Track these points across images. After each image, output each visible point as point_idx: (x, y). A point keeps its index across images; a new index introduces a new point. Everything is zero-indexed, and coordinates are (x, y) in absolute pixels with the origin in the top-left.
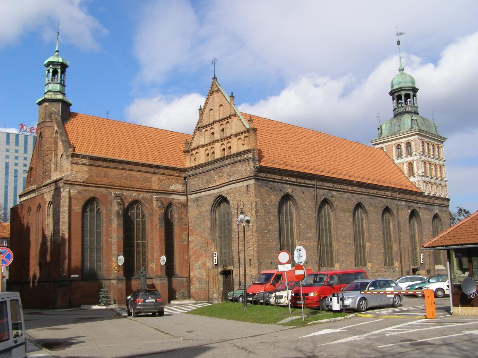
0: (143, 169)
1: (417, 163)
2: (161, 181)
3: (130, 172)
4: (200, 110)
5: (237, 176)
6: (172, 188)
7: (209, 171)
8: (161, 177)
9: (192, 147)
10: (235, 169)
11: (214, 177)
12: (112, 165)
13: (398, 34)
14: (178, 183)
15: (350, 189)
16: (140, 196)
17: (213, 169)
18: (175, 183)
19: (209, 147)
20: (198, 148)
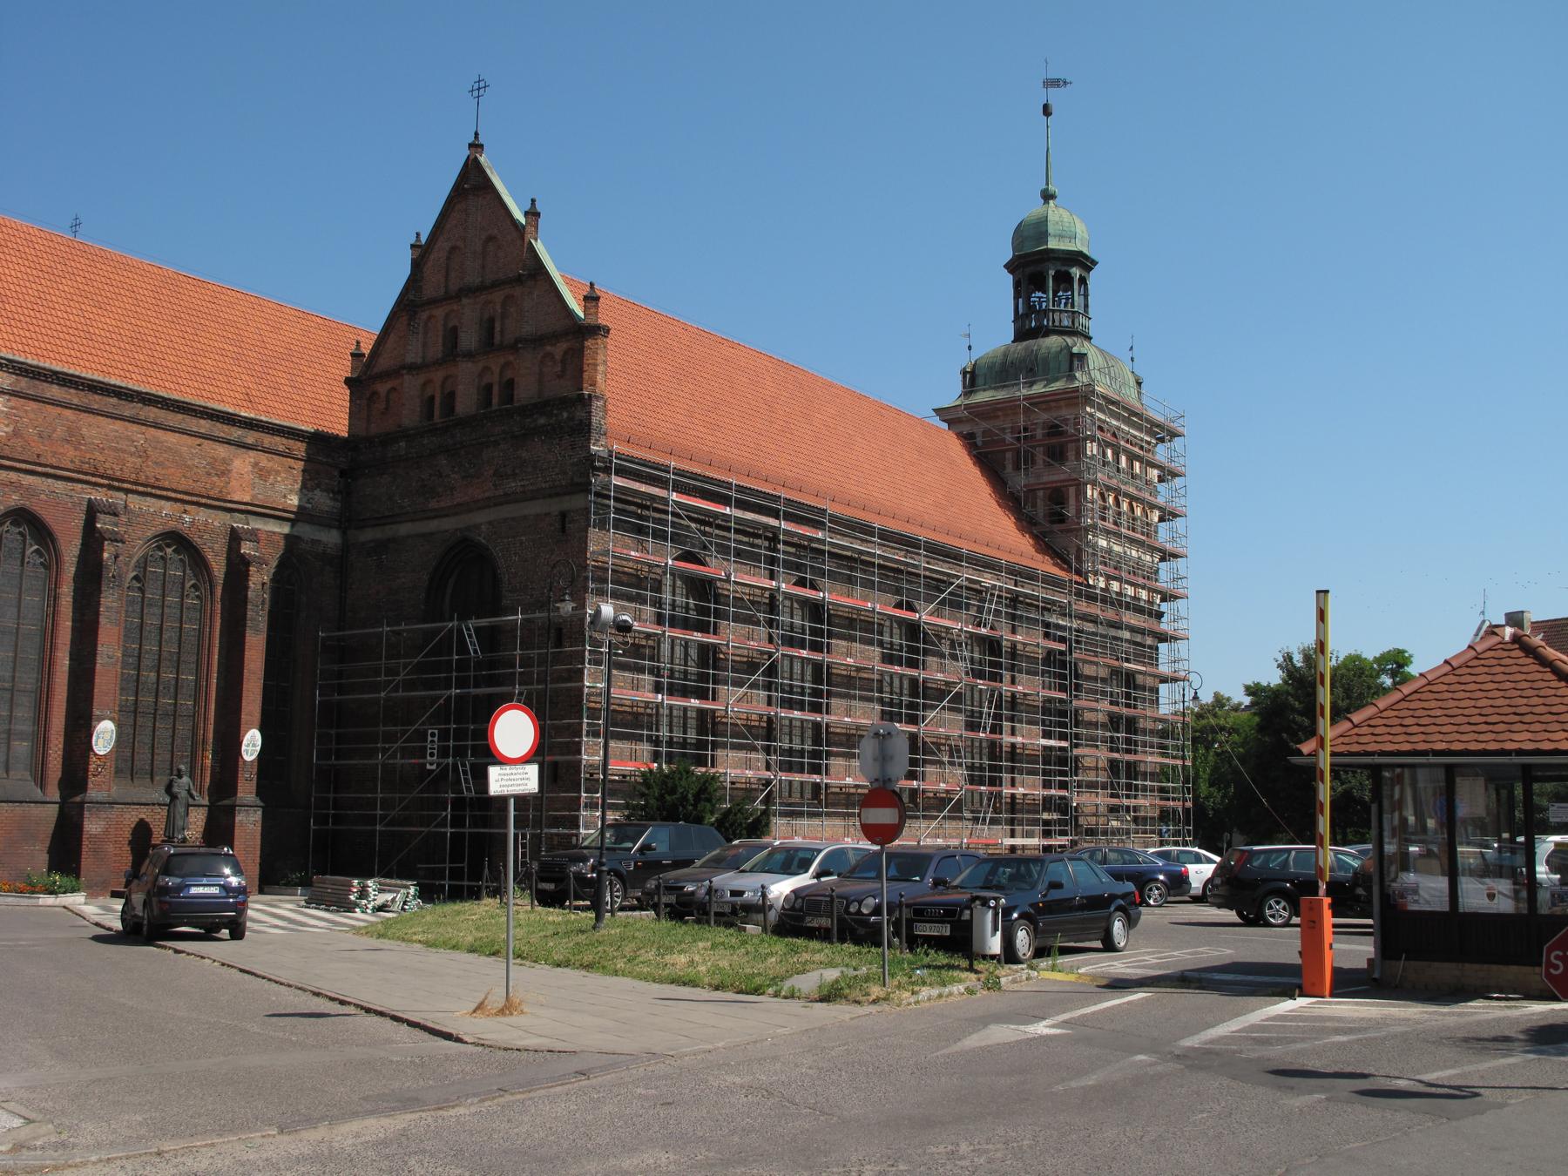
0: (204, 426)
2: (263, 474)
3: (160, 433)
8: (264, 460)
9: (376, 370)
12: (96, 401)
14: (318, 486)
19: (438, 375)
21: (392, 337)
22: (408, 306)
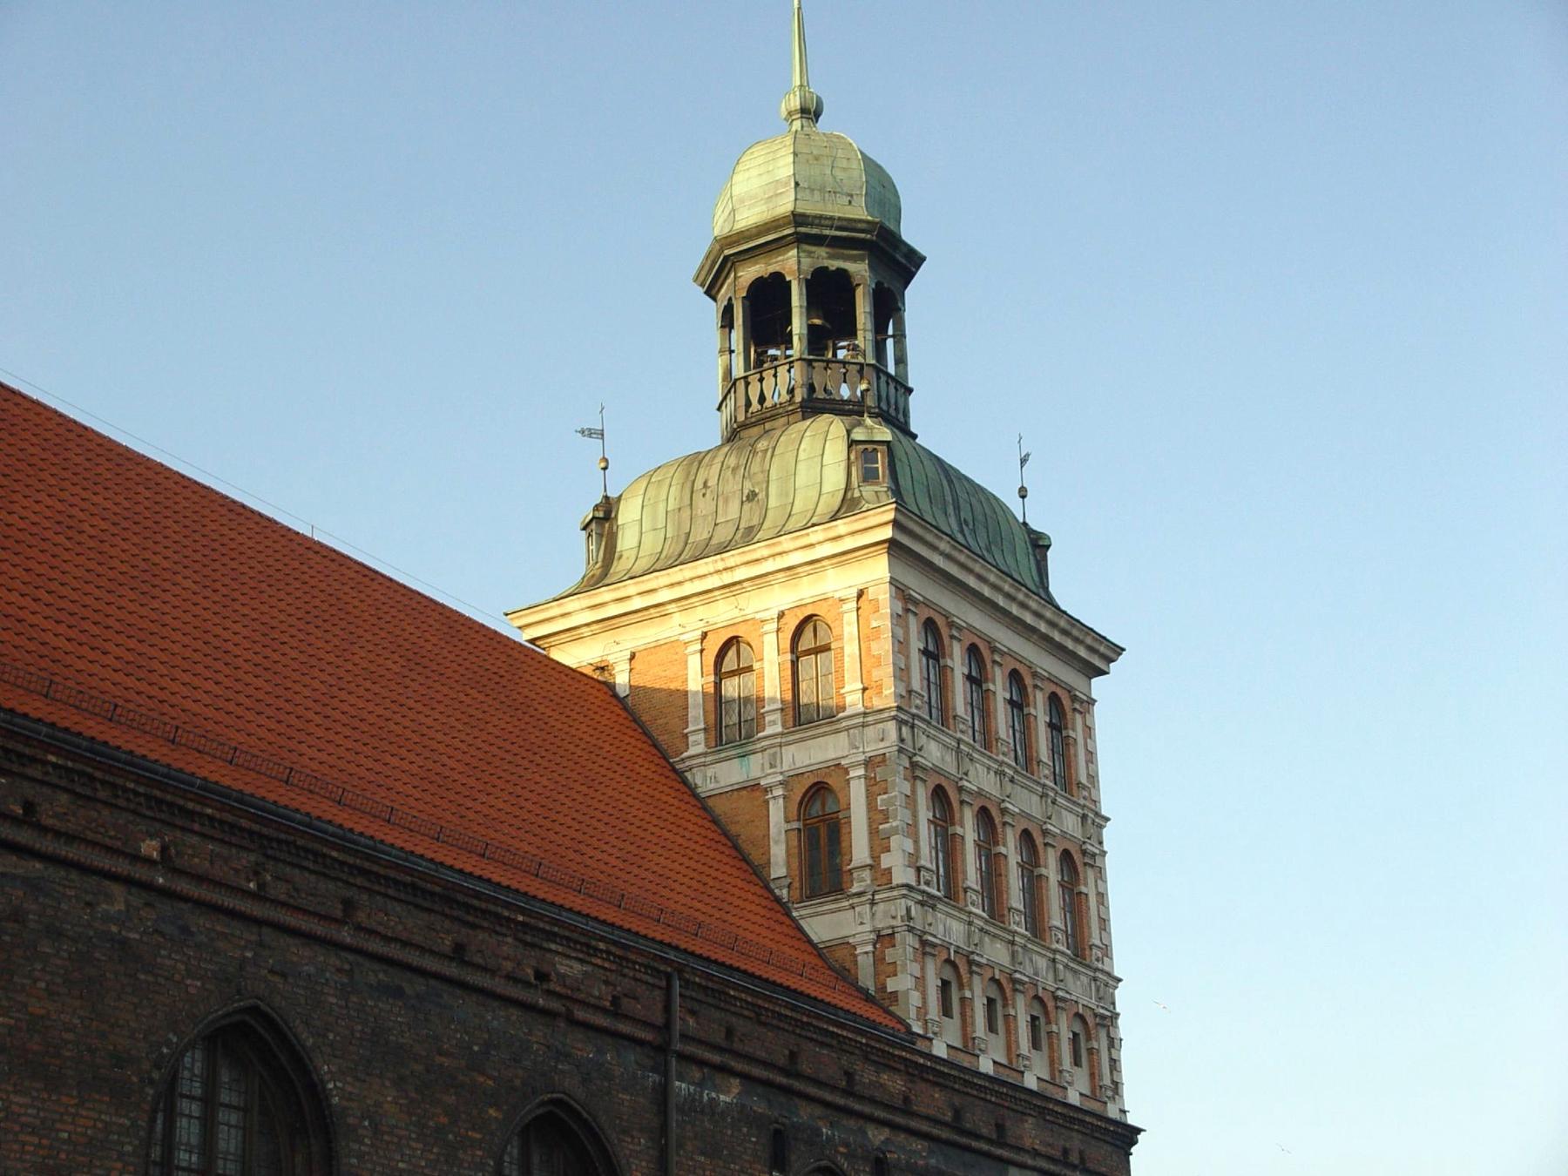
1: (874, 787)
15: (150, 848)
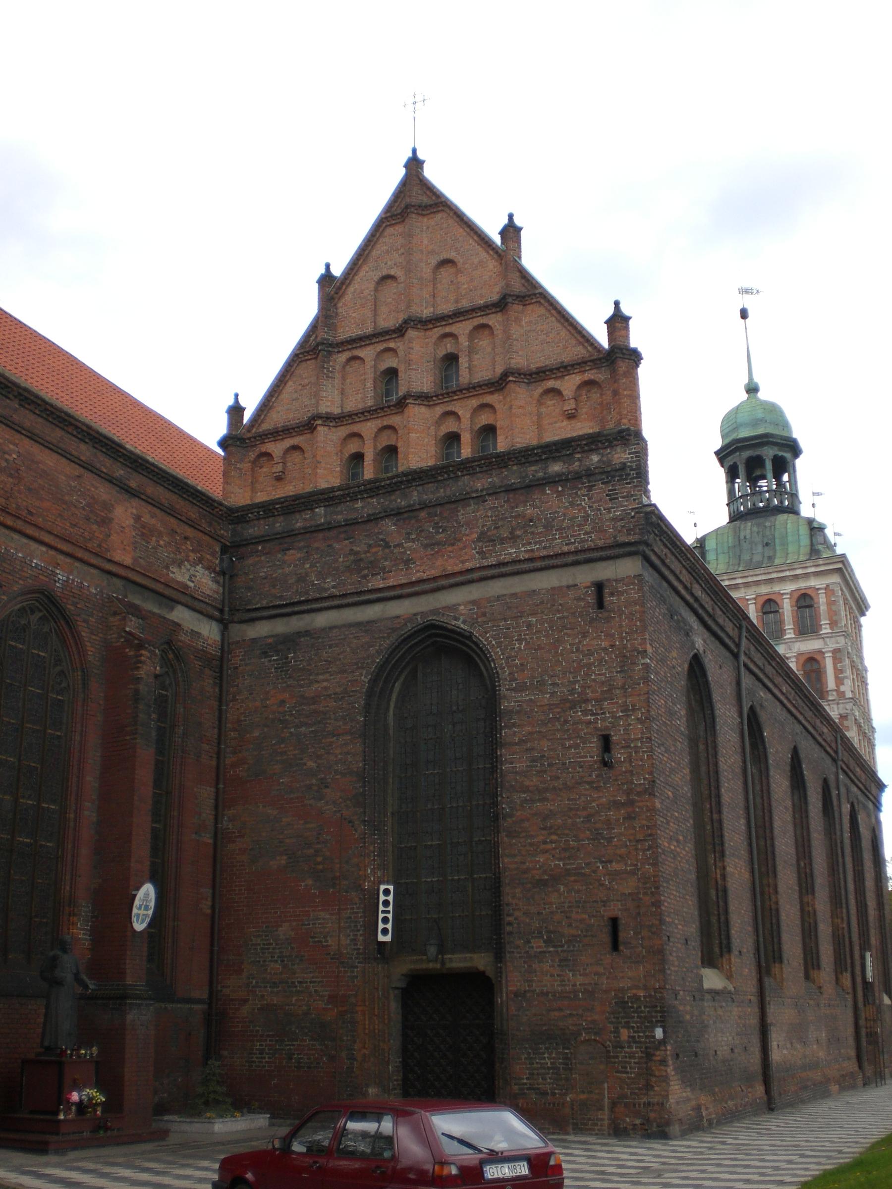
0: (85, 451)
2: (145, 532)
3: (36, 450)
4: (326, 279)
5: (540, 543)
6: (180, 575)
7: (373, 519)
9: (266, 426)
10: (529, 511)
11: (399, 545)
13: (746, 291)
14: (200, 561)
16: (61, 576)
17: (397, 514)
18: (192, 556)
19: (368, 428)
20: (309, 426)
21: (290, 386)
22: (316, 349)
